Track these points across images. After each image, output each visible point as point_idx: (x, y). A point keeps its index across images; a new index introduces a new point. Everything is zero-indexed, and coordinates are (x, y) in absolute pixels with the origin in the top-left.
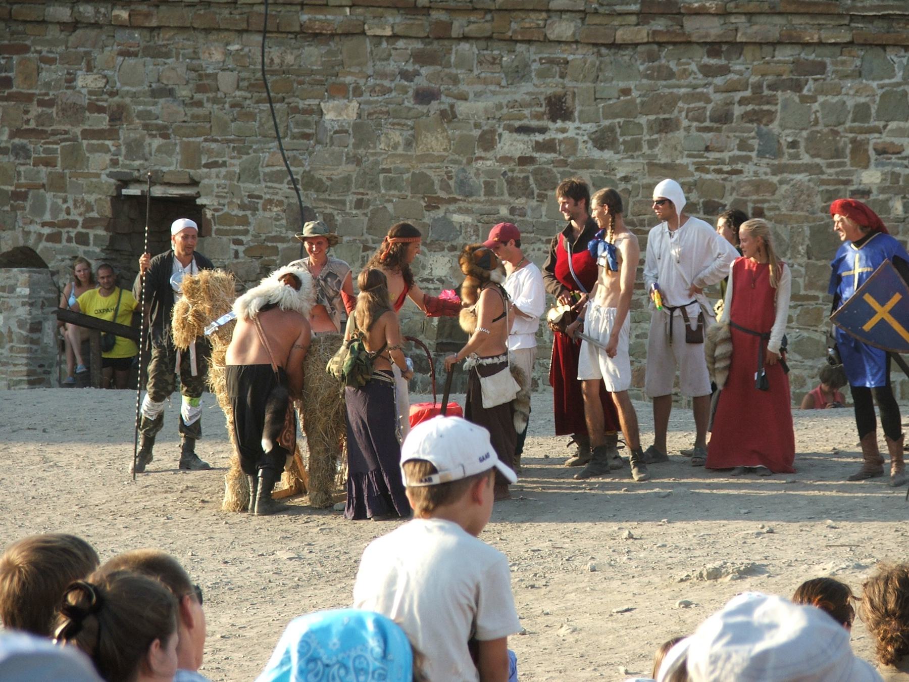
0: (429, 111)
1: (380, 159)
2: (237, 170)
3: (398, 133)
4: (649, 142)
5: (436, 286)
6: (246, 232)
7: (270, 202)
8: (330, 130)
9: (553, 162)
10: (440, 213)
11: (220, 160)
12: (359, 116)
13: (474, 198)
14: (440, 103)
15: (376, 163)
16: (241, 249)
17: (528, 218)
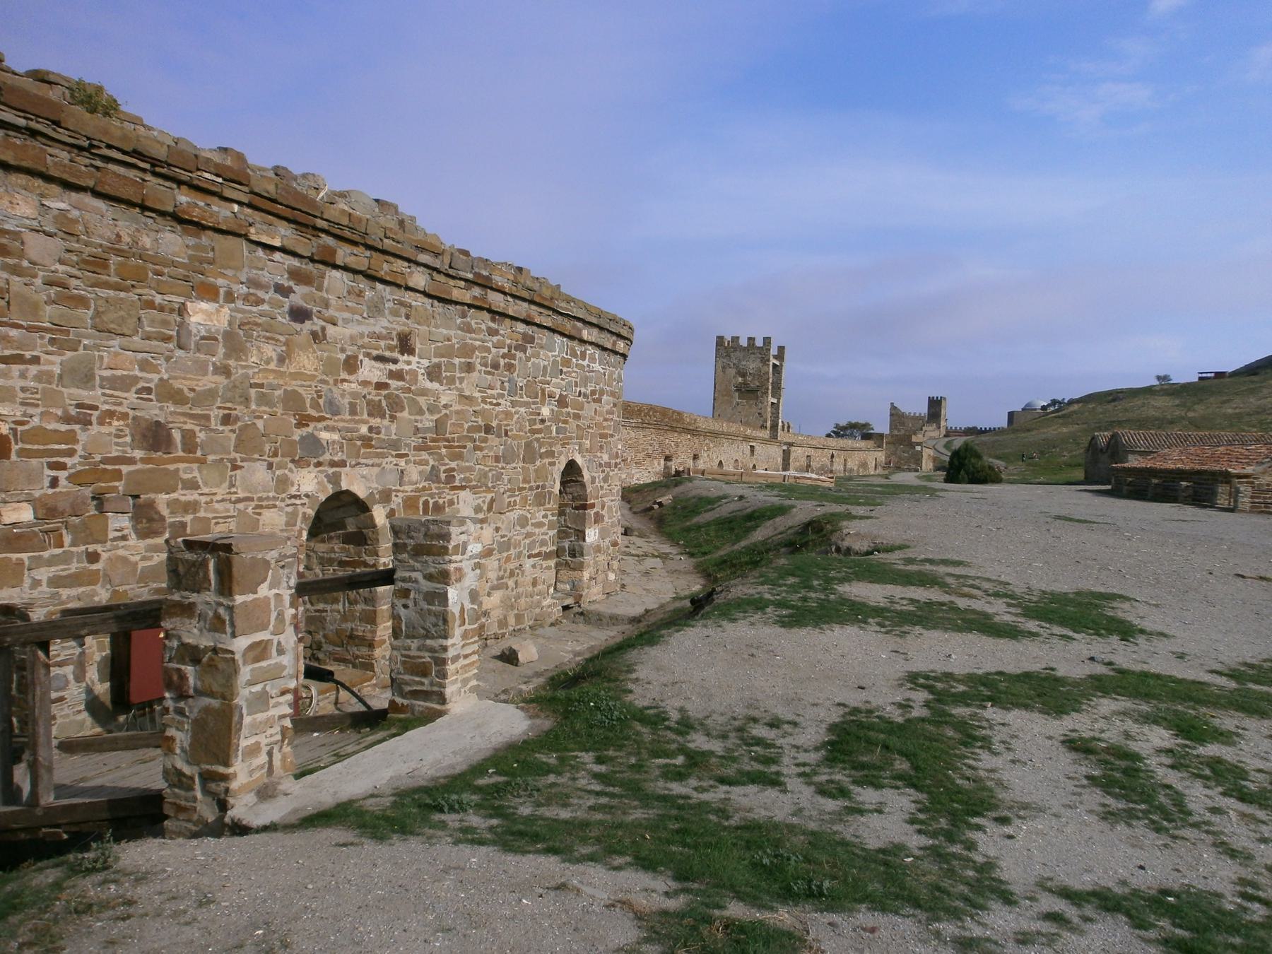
0: (301, 330)
1: (250, 372)
2: (57, 370)
3: (270, 347)
4: (459, 378)
5: (303, 501)
6: (71, 453)
7: (111, 414)
8: (195, 336)
9: (402, 389)
10: (310, 429)
11: (28, 355)
12: (230, 324)
13: (339, 417)
14: (314, 324)
15: (246, 376)
16: (62, 475)
17: (382, 436)
